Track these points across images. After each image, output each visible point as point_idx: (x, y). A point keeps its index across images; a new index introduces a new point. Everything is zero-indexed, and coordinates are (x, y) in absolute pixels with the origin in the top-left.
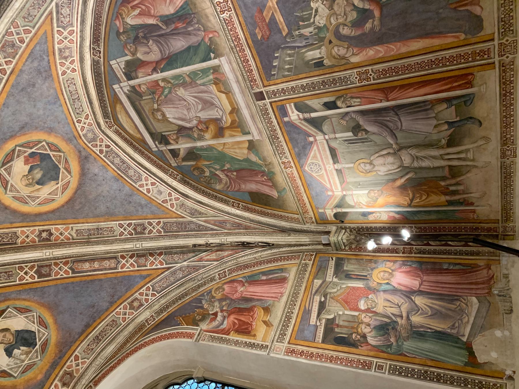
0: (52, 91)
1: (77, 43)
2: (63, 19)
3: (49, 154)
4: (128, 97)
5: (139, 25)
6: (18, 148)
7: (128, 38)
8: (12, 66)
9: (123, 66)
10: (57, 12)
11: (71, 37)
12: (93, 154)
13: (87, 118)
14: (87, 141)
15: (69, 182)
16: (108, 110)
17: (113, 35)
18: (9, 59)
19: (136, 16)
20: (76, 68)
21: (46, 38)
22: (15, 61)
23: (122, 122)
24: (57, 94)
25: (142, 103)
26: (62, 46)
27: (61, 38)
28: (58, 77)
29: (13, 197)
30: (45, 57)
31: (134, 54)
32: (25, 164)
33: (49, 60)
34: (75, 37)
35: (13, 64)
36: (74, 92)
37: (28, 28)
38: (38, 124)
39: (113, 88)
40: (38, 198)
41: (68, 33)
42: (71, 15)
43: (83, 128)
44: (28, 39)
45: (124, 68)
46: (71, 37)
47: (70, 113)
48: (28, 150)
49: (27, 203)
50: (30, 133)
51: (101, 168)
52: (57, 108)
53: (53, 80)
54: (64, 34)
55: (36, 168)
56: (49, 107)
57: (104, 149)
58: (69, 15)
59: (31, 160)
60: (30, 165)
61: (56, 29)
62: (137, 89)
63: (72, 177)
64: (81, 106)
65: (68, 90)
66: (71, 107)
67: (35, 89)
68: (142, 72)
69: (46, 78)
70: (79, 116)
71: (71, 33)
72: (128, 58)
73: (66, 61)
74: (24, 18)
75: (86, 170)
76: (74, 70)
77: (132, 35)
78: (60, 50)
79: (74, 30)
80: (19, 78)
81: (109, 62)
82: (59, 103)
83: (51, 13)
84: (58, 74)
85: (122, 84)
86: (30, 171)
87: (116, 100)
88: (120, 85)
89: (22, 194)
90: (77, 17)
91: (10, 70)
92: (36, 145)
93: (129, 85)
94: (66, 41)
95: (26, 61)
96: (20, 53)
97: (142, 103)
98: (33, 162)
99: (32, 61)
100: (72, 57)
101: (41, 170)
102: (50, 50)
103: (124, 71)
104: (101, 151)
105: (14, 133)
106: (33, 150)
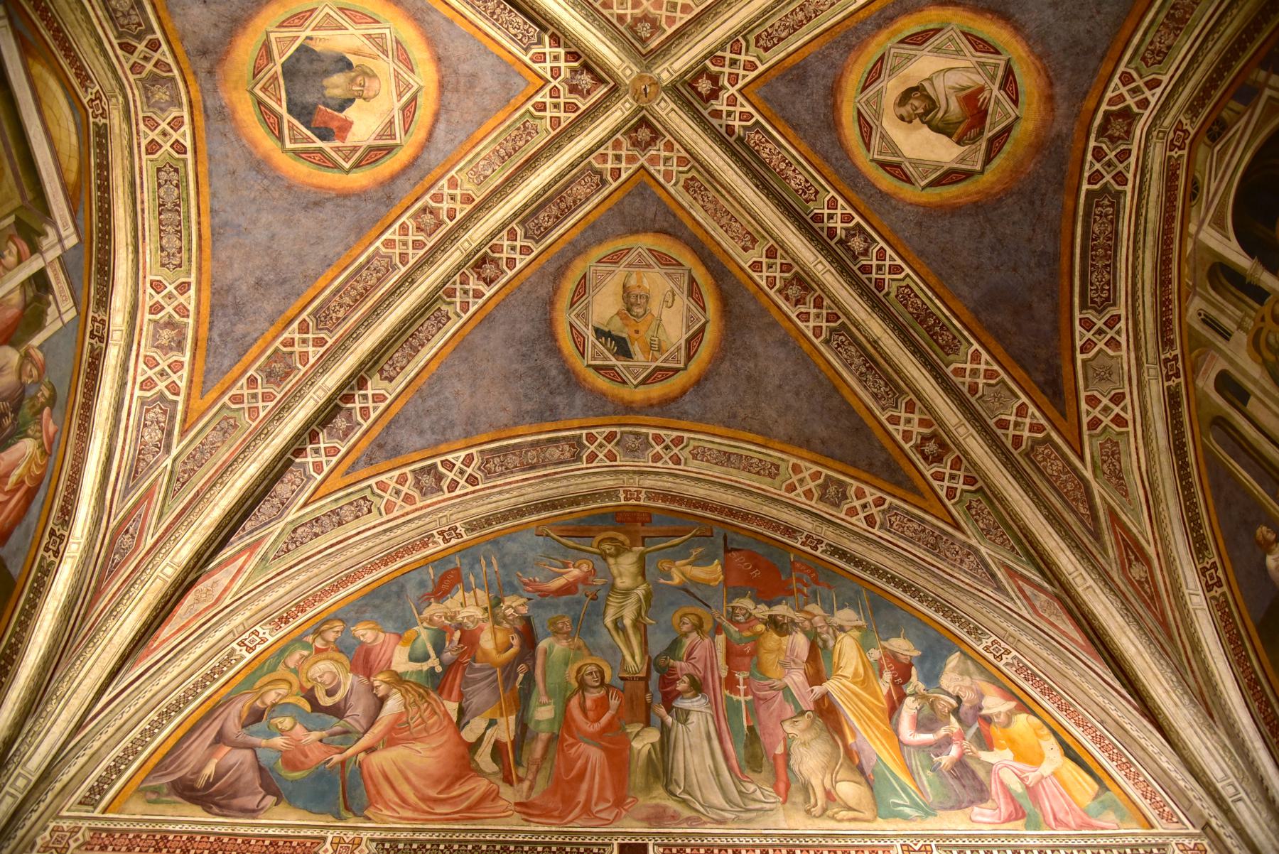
0: (223, 255)
1: (137, 356)
2: (161, 418)
3: (290, 111)
4: (46, 212)
5: (9, 446)
6: (347, 166)
7: (35, 397)
8: (286, 335)
9: (52, 310)
10: (170, 434)
11: (150, 373)
12: (179, 50)
13: (153, 147)
14: (176, 84)
15: (281, 26)
16: (97, 156)
17: (62, 392)
18: (285, 349)
19: (15, 466)
20: (150, 290)
21: (204, 382)
22: (277, 343)
23: (71, 118)
24: (213, 242)
25: (17, 202)
26: (176, 357)
27: (174, 377)
28: (199, 282)
29: (412, 71)
30: (217, 339)
31: (27, 357)
32: (351, 123)
33: (210, 329)
34: (139, 371)
35: (281, 339)
36: (170, 229)
37: (233, 406)
38: (281, 195)
39: (78, 235)
40: (369, 37)
41: (156, 385)
42: (143, 424)
43: (176, 124)
44: (239, 384)
45: (49, 304)
46: (150, 373)
47: (197, 182)
48: (328, 150)
49: (398, 42)
50: (308, 185)
51: (178, 10)
52: (225, 211)
53: (213, 280)
54: (166, 383)
55: (332, 98)
56: (242, 221)
57: (141, 47)
58: (145, 425)
59: (334, 125)
60: (342, 115)
61: (181, 399)
62: (25, 248)
63: (267, 34)
64: (160, 186)
65: (184, 242)
66: (188, 194)
67: (258, 273)
68: (12, 307)
69: (228, 291)
70: (173, 163)
71: (148, 384)
72: (37, 341)
73: (171, 316)
74: (235, 427)
75: (223, 26)
76: (157, 286)
77: (26, 411)
78: (180, 347)
79: (141, 389)
80: (282, 308)
81: (78, 313)
82: (217, 220)
83: (183, 433)
84: (199, 290)
85: (58, 251)
86: (350, 101)
87: (74, 197)
88: (63, 246)
89: (392, 65)
90: (128, 419)
91: (291, 329)
92: (306, 151)
93: (42, 253)
94: (163, 365)
95: (256, 340)
96: (263, 359)
97: (17, 202)
98: (333, 118)
99: (244, 336)
100: (156, 322)
101: (324, 88)
102: (201, 353)
103: (51, 297)
104: (155, 46)
105: (339, 201)
106: (319, 144)
